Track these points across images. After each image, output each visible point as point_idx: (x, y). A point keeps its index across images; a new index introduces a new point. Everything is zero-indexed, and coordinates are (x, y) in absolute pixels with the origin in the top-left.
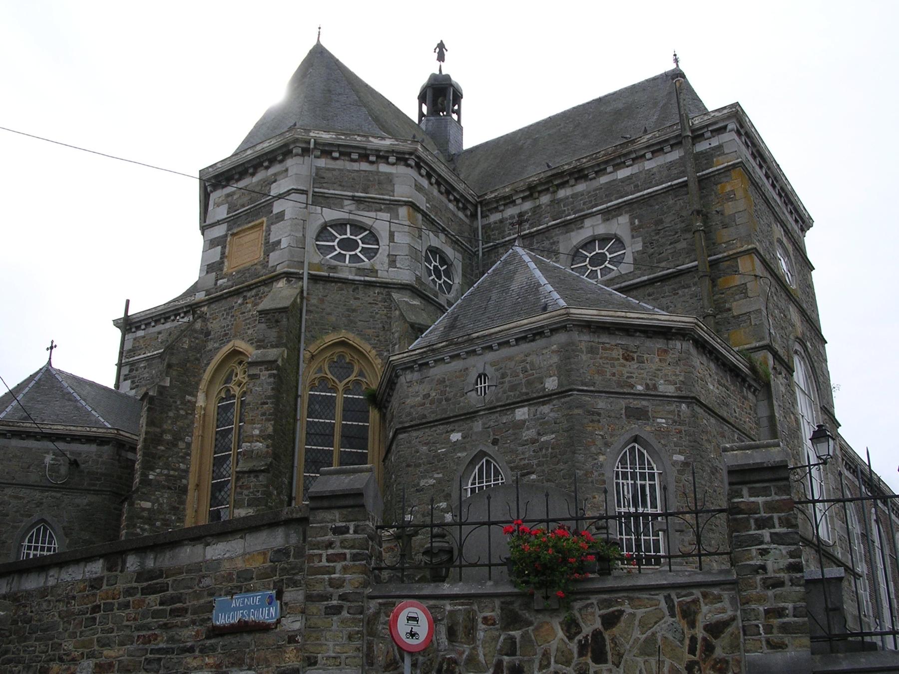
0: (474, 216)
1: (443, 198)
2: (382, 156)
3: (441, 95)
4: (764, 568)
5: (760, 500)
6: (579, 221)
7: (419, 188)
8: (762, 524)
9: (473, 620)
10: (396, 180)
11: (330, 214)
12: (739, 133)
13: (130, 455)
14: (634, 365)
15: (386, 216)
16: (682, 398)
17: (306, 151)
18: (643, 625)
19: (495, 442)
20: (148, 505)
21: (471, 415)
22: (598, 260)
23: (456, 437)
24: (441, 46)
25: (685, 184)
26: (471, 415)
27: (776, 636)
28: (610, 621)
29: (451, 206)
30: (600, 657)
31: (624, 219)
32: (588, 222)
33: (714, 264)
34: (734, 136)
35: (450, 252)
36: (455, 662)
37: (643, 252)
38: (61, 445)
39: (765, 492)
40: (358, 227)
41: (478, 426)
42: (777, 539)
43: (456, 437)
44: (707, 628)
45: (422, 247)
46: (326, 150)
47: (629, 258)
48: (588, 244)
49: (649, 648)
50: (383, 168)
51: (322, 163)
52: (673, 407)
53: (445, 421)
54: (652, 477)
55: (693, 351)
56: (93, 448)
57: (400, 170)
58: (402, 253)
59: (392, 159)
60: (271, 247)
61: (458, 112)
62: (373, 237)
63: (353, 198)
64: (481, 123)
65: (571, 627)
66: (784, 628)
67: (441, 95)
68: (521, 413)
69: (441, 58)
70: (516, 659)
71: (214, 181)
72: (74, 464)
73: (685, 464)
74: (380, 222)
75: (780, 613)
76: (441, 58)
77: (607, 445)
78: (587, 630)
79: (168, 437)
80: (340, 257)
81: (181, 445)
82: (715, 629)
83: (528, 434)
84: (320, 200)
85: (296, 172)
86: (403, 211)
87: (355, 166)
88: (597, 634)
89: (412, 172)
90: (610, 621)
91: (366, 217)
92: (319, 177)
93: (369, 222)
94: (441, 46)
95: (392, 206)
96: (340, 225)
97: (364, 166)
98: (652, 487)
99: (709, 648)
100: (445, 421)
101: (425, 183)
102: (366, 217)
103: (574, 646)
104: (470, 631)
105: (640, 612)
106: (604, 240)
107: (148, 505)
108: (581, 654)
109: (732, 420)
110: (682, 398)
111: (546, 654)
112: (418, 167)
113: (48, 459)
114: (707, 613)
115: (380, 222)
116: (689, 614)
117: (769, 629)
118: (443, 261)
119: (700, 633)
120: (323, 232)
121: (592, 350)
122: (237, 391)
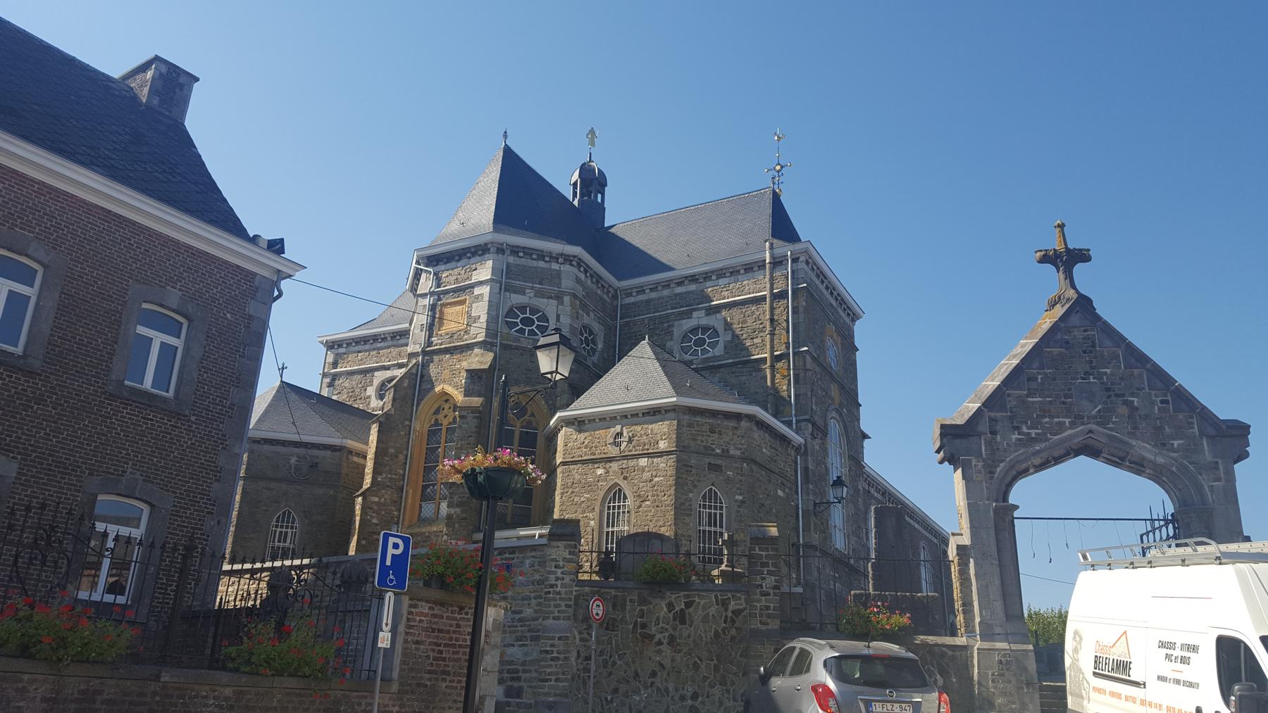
0: (615, 297)
1: (594, 286)
2: (554, 258)
3: (592, 182)
4: (761, 586)
5: (764, 553)
6: (688, 315)
7: (578, 280)
8: (764, 565)
9: (625, 600)
10: (563, 276)
11: (516, 299)
12: (807, 263)
13: (360, 461)
14: (716, 436)
15: (555, 302)
16: (744, 459)
18: (704, 608)
19: (625, 478)
20: (376, 499)
21: (610, 460)
22: (700, 342)
23: (600, 472)
25: (764, 298)
26: (610, 460)
27: (764, 619)
28: (688, 605)
29: (599, 292)
30: (683, 622)
32: (695, 314)
34: (805, 266)
35: (596, 327)
36: (614, 620)
37: (731, 342)
38: (302, 451)
39: (767, 550)
41: (615, 466)
42: (769, 573)
43: (600, 472)
44: (733, 612)
45: (577, 325)
46: (515, 250)
47: (721, 346)
48: (694, 331)
49: (705, 619)
50: (555, 266)
51: (511, 259)
52: (738, 465)
53: (593, 461)
54: (721, 508)
55: (755, 428)
56: (329, 453)
57: (566, 268)
59: (561, 260)
60: (472, 320)
62: (544, 318)
63: (532, 288)
65: (670, 606)
66: (769, 616)
67: (592, 182)
68: (643, 462)
70: (644, 620)
72: (314, 466)
73: (743, 502)
74: (550, 307)
75: (768, 608)
77: (695, 486)
78: (677, 609)
79: (392, 451)
80: (521, 331)
81: (401, 457)
82: (737, 613)
83: (647, 475)
84: (509, 289)
87: (534, 263)
88: (682, 610)
89: (575, 270)
90: (688, 605)
91: (541, 303)
93: (543, 307)
95: (559, 298)
96: (522, 309)
97: (541, 264)
98: (721, 515)
99: (733, 621)
100: (593, 461)
101: (582, 276)
102: (541, 303)
103: (671, 615)
104: (624, 608)
105: (702, 602)
106: (705, 329)
107: (376, 499)
108: (674, 619)
109: (777, 470)
110: (744, 459)
111: (658, 618)
112: (579, 266)
113: (293, 461)
114: (733, 605)
115: (550, 307)
116: (724, 604)
117: (761, 615)
118: (591, 333)
119: (730, 614)
120: (510, 313)
121: (690, 425)
122: (445, 422)
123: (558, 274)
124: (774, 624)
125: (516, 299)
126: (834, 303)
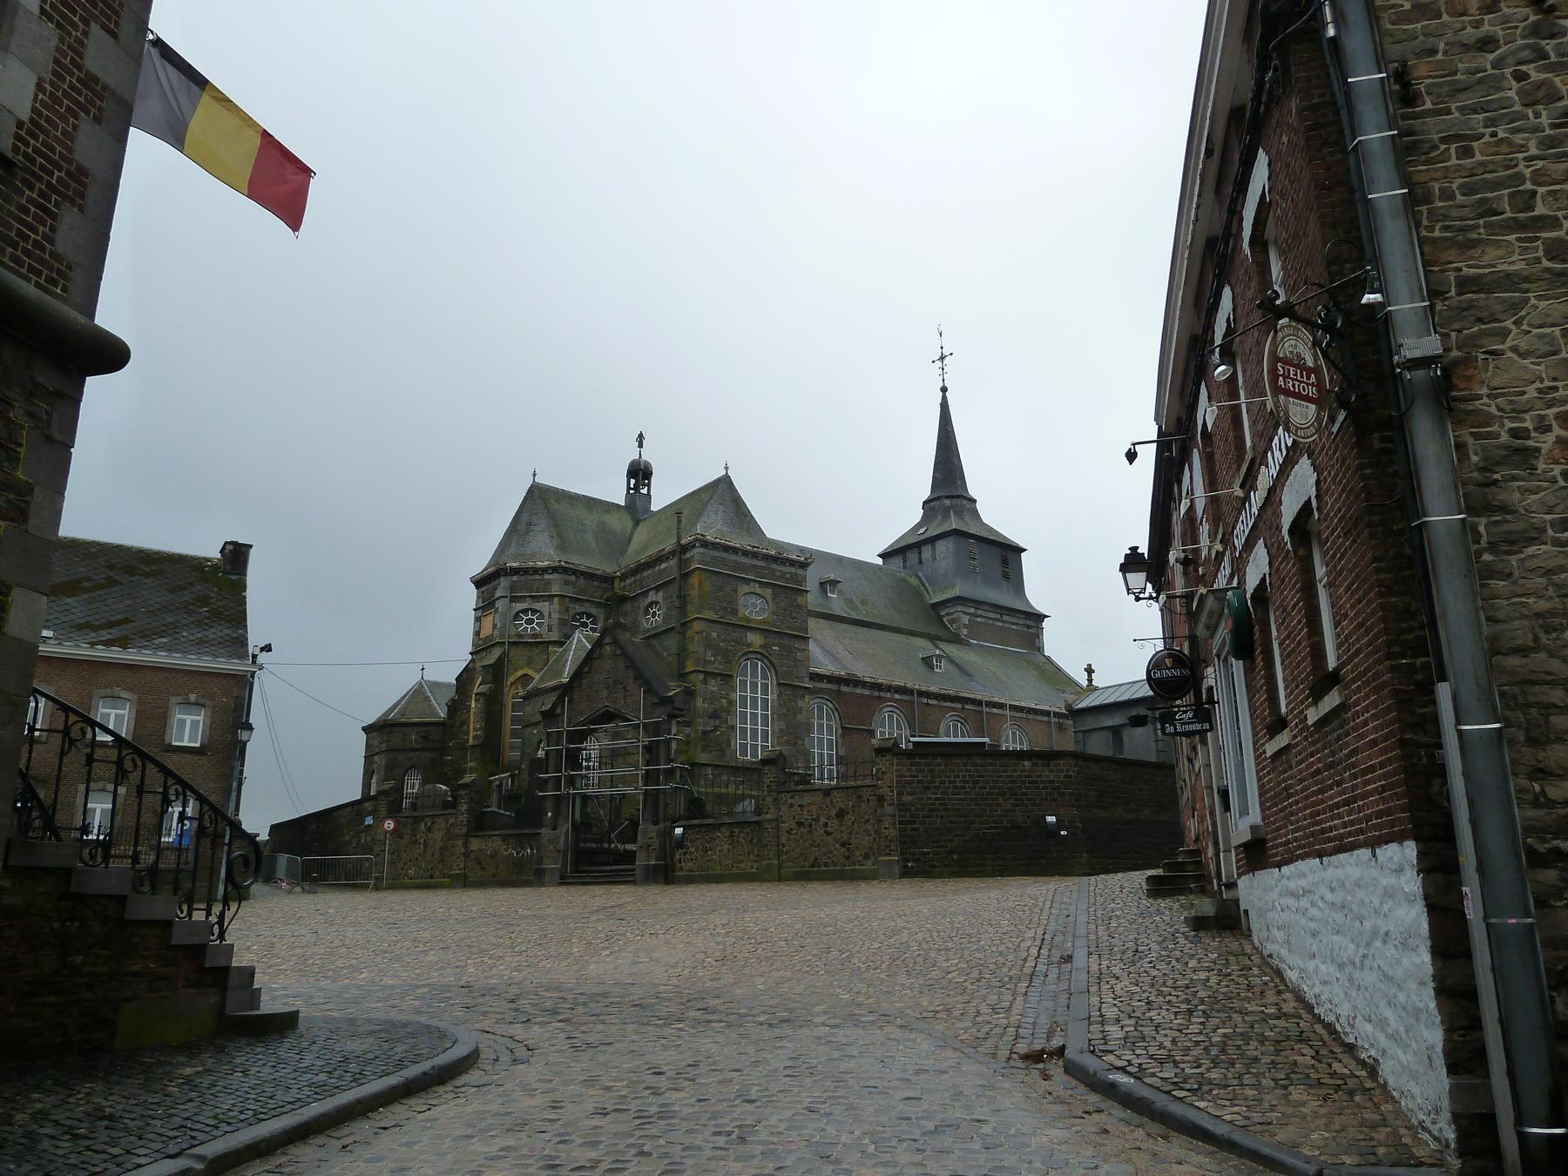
2: (545, 570)
3: (640, 473)
7: (567, 583)
11: (520, 606)
17: (506, 574)
24: (641, 436)
31: (661, 594)
33: (684, 624)
40: (534, 611)
50: (546, 576)
57: (555, 576)
58: (555, 622)
61: (649, 485)
62: (542, 616)
64: (663, 494)
67: (640, 473)
69: (641, 446)
71: (479, 582)
74: (543, 606)
76: (641, 446)
84: (513, 599)
85: (504, 582)
86: (556, 600)
91: (538, 606)
92: (512, 589)
94: (641, 436)
96: (525, 611)
102: (538, 606)
123: (549, 582)
124: (465, 830)
125: (520, 606)
126: (761, 563)
